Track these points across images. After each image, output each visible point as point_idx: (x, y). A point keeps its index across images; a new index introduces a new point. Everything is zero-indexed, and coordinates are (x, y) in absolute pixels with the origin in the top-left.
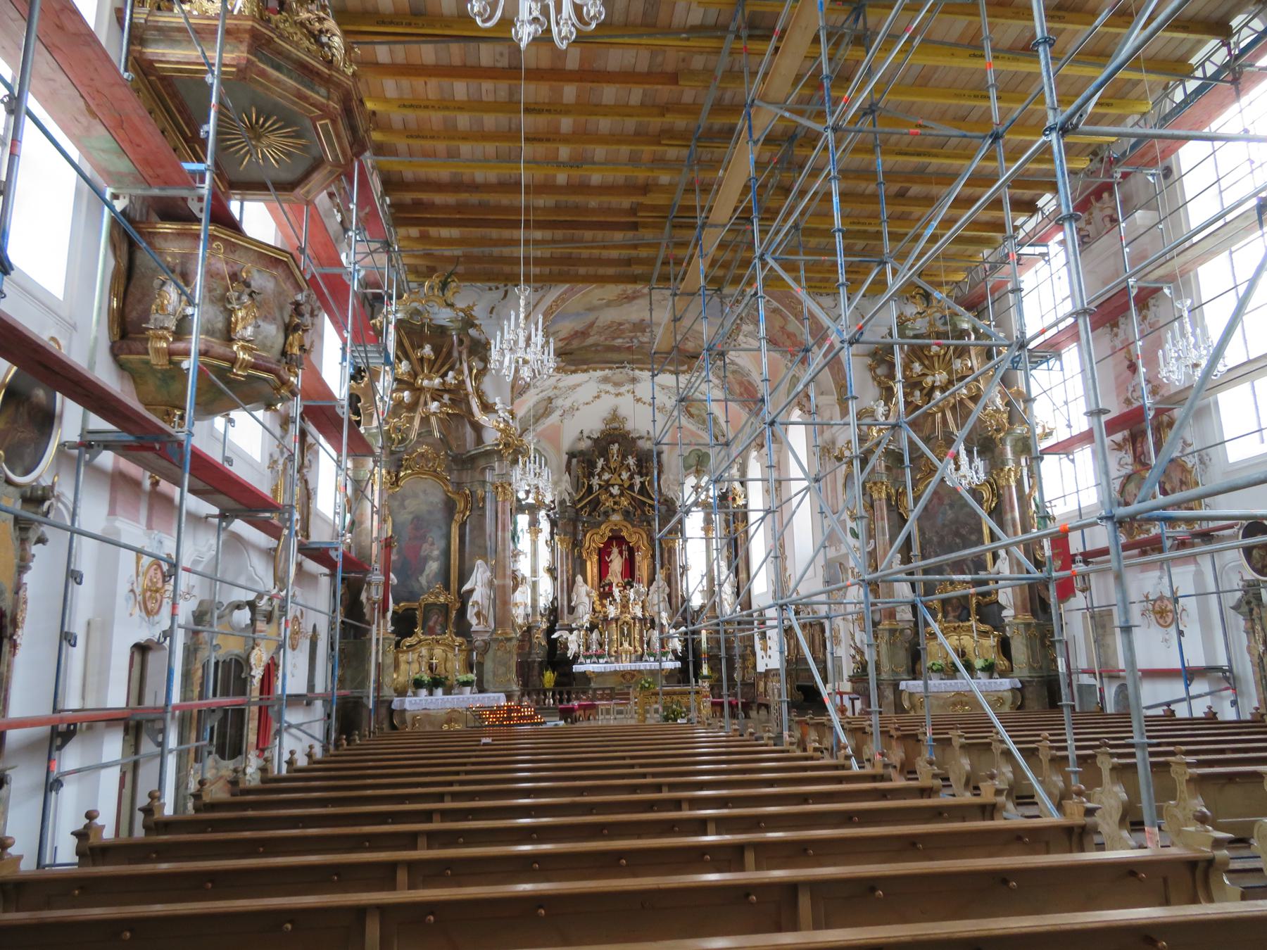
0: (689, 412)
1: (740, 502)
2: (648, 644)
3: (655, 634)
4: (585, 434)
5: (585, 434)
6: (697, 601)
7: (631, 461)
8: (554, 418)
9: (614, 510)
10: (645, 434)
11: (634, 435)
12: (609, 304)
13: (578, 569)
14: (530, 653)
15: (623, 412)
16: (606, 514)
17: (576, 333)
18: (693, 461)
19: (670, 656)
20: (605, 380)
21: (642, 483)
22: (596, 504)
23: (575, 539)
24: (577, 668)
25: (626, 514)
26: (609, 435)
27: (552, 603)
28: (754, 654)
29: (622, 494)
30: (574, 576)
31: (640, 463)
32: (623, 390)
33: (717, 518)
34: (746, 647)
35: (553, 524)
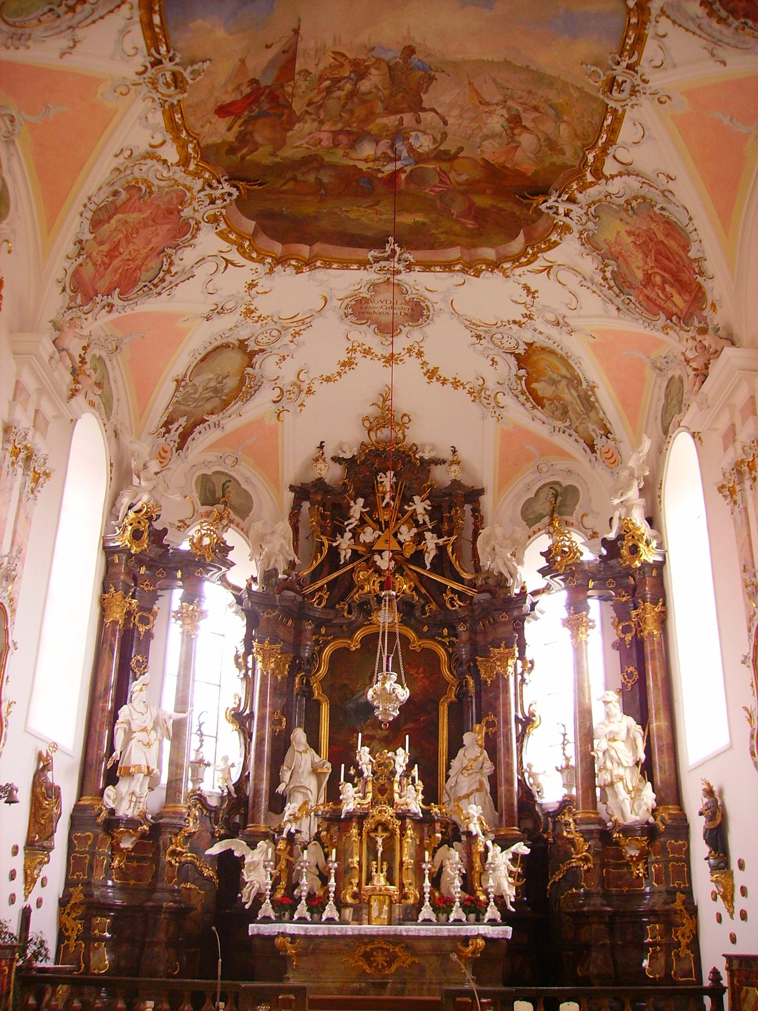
0: (533, 392)
2: (436, 881)
3: (453, 858)
4: (329, 452)
6: (552, 792)
8: (260, 405)
10: (447, 455)
11: (427, 456)
16: (366, 608)
19: (492, 912)
20: (358, 310)
21: (441, 549)
22: (343, 588)
25: (406, 608)
27: (240, 786)
28: (693, 911)
29: (399, 569)
30: (289, 730)
32: (401, 343)
34: (671, 893)
35: (253, 622)
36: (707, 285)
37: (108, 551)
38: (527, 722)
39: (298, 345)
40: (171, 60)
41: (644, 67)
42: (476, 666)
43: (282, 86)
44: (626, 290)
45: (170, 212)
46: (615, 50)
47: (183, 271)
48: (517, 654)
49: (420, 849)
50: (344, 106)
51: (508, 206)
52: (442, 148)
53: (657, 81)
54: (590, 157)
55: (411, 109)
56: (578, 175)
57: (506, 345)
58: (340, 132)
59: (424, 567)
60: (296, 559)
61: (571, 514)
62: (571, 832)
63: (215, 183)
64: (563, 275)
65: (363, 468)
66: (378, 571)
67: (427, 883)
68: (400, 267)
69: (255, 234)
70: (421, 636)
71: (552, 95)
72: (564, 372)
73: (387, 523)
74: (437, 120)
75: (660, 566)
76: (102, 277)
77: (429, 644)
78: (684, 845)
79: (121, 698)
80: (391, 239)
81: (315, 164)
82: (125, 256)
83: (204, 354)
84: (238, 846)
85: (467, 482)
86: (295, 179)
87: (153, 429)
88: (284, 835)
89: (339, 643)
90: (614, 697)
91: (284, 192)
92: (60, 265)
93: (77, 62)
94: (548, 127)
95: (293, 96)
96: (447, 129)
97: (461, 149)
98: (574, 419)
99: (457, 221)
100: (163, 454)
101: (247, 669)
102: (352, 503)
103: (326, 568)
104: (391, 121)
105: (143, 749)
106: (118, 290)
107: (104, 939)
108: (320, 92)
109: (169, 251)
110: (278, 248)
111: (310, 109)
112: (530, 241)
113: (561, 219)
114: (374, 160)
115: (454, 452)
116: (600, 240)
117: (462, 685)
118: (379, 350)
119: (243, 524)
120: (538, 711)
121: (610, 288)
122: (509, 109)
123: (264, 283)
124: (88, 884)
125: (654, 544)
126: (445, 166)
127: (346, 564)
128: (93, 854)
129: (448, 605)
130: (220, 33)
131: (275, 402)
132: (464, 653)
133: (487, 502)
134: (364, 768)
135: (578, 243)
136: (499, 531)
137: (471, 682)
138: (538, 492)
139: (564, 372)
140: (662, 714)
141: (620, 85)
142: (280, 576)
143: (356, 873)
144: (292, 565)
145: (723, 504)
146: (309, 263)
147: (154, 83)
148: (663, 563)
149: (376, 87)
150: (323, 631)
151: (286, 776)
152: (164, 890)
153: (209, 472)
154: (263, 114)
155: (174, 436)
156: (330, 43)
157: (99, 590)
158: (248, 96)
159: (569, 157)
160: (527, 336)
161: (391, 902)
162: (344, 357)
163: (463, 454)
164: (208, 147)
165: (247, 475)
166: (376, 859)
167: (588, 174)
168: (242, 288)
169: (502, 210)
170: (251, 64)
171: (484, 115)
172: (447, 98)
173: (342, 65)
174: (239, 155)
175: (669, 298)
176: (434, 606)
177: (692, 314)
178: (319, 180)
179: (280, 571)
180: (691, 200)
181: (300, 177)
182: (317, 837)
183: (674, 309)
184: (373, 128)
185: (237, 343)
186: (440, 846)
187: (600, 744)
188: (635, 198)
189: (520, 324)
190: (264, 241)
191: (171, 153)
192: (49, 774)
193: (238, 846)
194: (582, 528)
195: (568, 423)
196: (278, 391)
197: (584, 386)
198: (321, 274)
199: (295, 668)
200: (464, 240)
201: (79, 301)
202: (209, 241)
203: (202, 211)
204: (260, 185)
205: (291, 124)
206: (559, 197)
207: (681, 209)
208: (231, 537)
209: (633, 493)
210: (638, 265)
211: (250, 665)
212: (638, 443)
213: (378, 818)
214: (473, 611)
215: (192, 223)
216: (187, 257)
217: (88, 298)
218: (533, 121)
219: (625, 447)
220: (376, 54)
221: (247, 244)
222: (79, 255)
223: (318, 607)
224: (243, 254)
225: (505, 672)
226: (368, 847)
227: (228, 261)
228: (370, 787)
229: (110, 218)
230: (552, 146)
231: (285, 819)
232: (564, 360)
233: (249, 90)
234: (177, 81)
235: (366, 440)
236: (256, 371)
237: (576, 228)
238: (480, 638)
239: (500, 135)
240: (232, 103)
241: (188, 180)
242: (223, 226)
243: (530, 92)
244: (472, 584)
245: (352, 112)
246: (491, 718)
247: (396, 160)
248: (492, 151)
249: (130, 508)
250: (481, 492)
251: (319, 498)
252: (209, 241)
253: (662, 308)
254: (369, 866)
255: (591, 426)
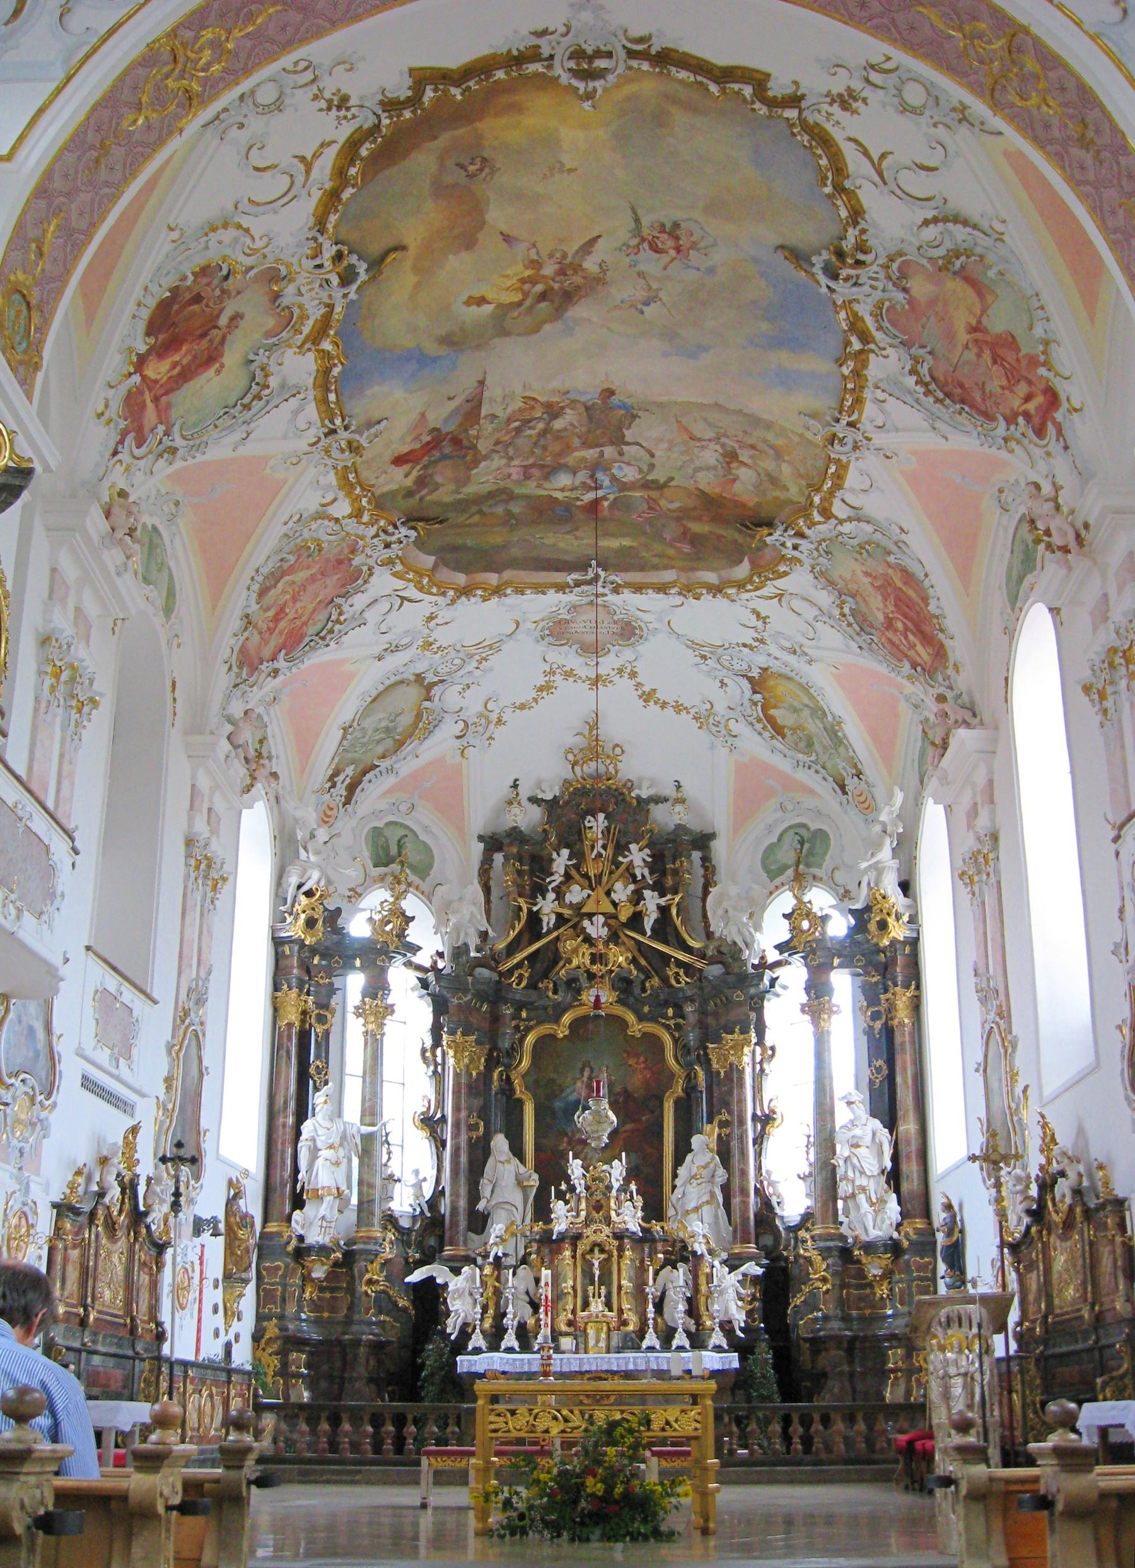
1: (898, 931)
2: (659, 1306)
4: (525, 792)
5: (525, 792)
7: (638, 857)
8: (440, 743)
9: (591, 976)
10: (669, 791)
11: (644, 795)
12: (501, 324)
13: (497, 1120)
14: (348, 1322)
15: (612, 731)
16: (573, 985)
17: (437, 439)
18: (786, 855)
21: (664, 910)
22: (546, 962)
23: (494, 1047)
24: (464, 1363)
25: (624, 986)
26: (582, 792)
29: (614, 938)
31: (657, 863)
33: (843, 984)
35: (440, 1007)
36: (947, 643)
37: (278, 942)
38: (766, 1120)
39: (484, 671)
40: (346, 428)
41: (866, 425)
42: (706, 1054)
43: (466, 431)
44: (868, 629)
45: (340, 562)
46: (833, 405)
47: (353, 617)
48: (754, 1040)
49: (642, 1270)
50: (535, 443)
51: (730, 534)
52: (649, 478)
53: (878, 439)
54: (817, 500)
55: (612, 443)
56: (805, 510)
57: (737, 667)
58: (532, 466)
59: (644, 933)
60: (490, 931)
61: (820, 866)
62: (807, 1250)
63: (390, 529)
64: (796, 604)
65: (567, 813)
66: (588, 940)
67: (650, 1307)
68: (606, 591)
69: (435, 566)
70: (641, 1018)
71: (770, 436)
72: (806, 701)
73: (599, 877)
74: (643, 453)
75: (914, 943)
76: (267, 642)
77: (650, 1027)
78: (929, 1263)
79: (302, 1112)
80: (594, 563)
81: (504, 497)
82: (291, 616)
83: (374, 693)
84: (439, 1272)
85: (695, 825)
86: (480, 512)
87: (317, 787)
88: (491, 1260)
89: (545, 1029)
90: (861, 1098)
91: (470, 525)
92: (228, 643)
93: (250, 449)
94: (768, 464)
95: (478, 438)
96: (653, 461)
97: (672, 479)
98: (820, 751)
99: (672, 546)
100: (329, 813)
101: (436, 1065)
102: (555, 855)
103: (526, 937)
104: (591, 454)
105: (326, 1169)
106: (283, 652)
107: (301, 1375)
108: (508, 433)
109: (339, 601)
110: (461, 579)
111: (498, 448)
112: (757, 568)
113: (789, 552)
114: (572, 490)
115: (679, 787)
116: (834, 575)
117: (690, 1078)
118: (583, 672)
119: (423, 886)
120: (780, 1107)
121: (850, 625)
122: (723, 446)
123: (444, 615)
124: (281, 1317)
125: (906, 918)
126: (654, 494)
127: (549, 932)
128: (285, 1286)
129: (673, 982)
130: (399, 394)
131: (458, 737)
132: (692, 1037)
133: (719, 848)
134: (576, 1182)
135: (811, 576)
136: (733, 890)
137: (701, 1075)
138: (781, 835)
139: (806, 701)
140: (911, 1116)
141: (841, 440)
142: (473, 954)
143: (570, 1298)
144: (484, 935)
145: (964, 891)
146: (498, 591)
147: (327, 452)
148: (917, 939)
149: (572, 425)
150: (524, 1014)
151: (485, 1188)
152: (362, 1322)
153: (380, 824)
154: (444, 457)
155: (341, 790)
156: (519, 391)
157: (270, 988)
158: (428, 443)
159: (794, 492)
160: (761, 660)
161: (609, 1329)
162: (541, 681)
163: (688, 790)
164: (383, 495)
165: (426, 822)
166: (592, 1283)
167: (815, 513)
168: (419, 622)
169: (720, 537)
170: (431, 417)
171: (696, 451)
172: (655, 434)
173: (533, 408)
174: (417, 497)
175: (912, 647)
176: (656, 981)
177: (936, 669)
178: (508, 513)
179: (472, 948)
180: (926, 552)
181: (485, 509)
182: (524, 1261)
183: (919, 660)
184: (570, 460)
185: (412, 678)
186: (662, 1267)
187: (842, 1150)
188: (869, 543)
189: (751, 648)
190: (445, 574)
191: (342, 508)
192: (241, 1202)
193: (439, 1272)
194: (832, 885)
195: (813, 758)
196: (461, 725)
197: (830, 718)
198: (512, 599)
199: (492, 1062)
200: (679, 564)
201: (244, 676)
202: (383, 582)
203: (375, 556)
204: (441, 522)
205: (476, 463)
206: (786, 530)
207: (916, 562)
208: (412, 904)
209: (885, 854)
210: (877, 607)
211: (439, 1060)
212: (891, 796)
213: (593, 1238)
214: (701, 989)
215: (365, 568)
216: (359, 601)
217: (254, 669)
218: (751, 457)
219: (879, 793)
220: (571, 396)
221: (425, 581)
222: (246, 629)
223: (518, 985)
224: (421, 589)
225: (740, 1062)
226: (583, 1271)
227: (403, 598)
228: (583, 1205)
229: (278, 581)
230: (774, 481)
231: (491, 1241)
232: (805, 689)
233: (429, 438)
234: (353, 448)
235: (569, 775)
236: (435, 704)
237: (807, 562)
238: (710, 1020)
239: (715, 468)
240: (411, 452)
241: (361, 530)
242: (399, 567)
243: (745, 432)
244: (702, 955)
245: (545, 448)
246: (725, 1116)
247: (596, 489)
248: (707, 482)
249: (299, 887)
250: (712, 836)
251: (515, 850)
252: (383, 582)
253: (906, 656)
254: (585, 1292)
255: (841, 765)
